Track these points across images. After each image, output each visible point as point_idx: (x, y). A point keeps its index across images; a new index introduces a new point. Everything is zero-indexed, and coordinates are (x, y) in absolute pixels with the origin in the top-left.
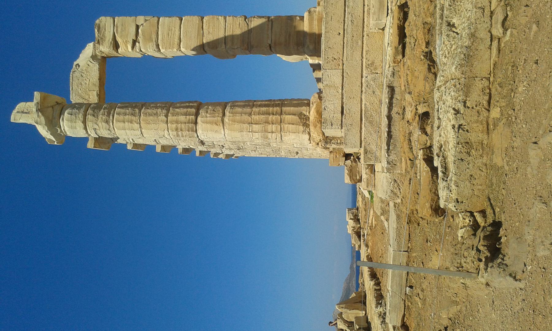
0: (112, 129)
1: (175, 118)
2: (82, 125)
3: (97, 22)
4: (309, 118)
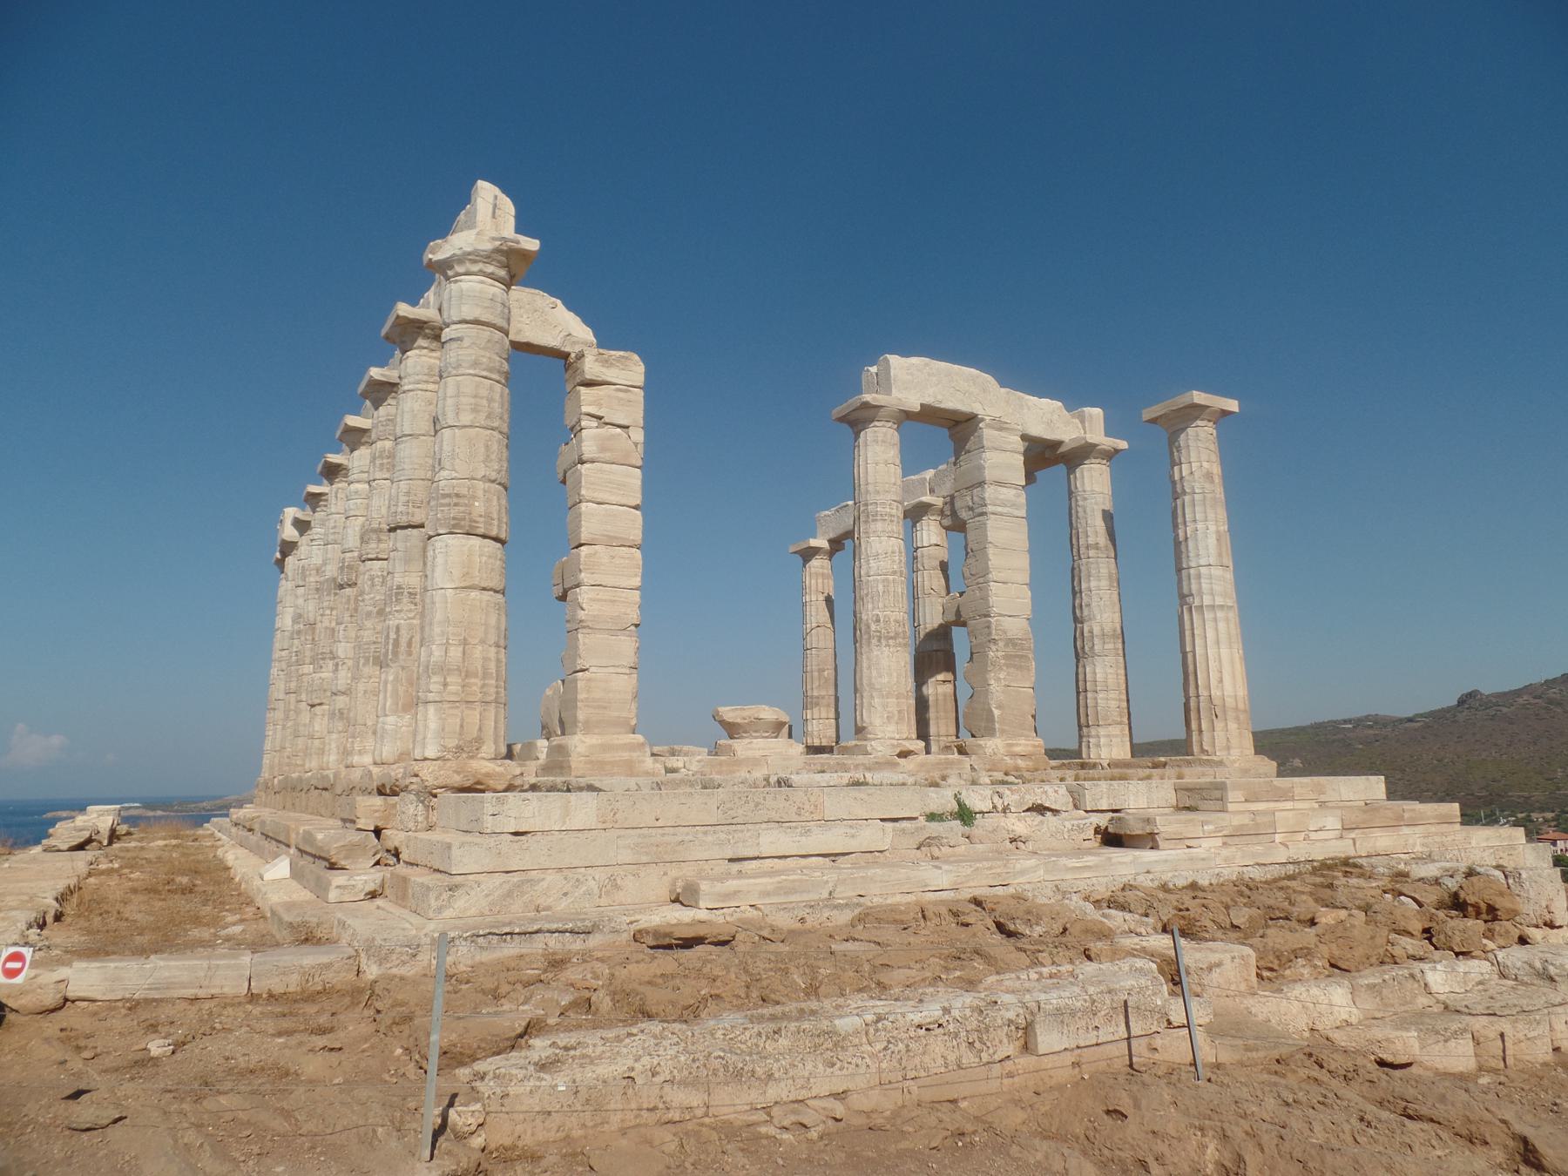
1: (480, 493)
3: (636, 357)
4: (472, 757)
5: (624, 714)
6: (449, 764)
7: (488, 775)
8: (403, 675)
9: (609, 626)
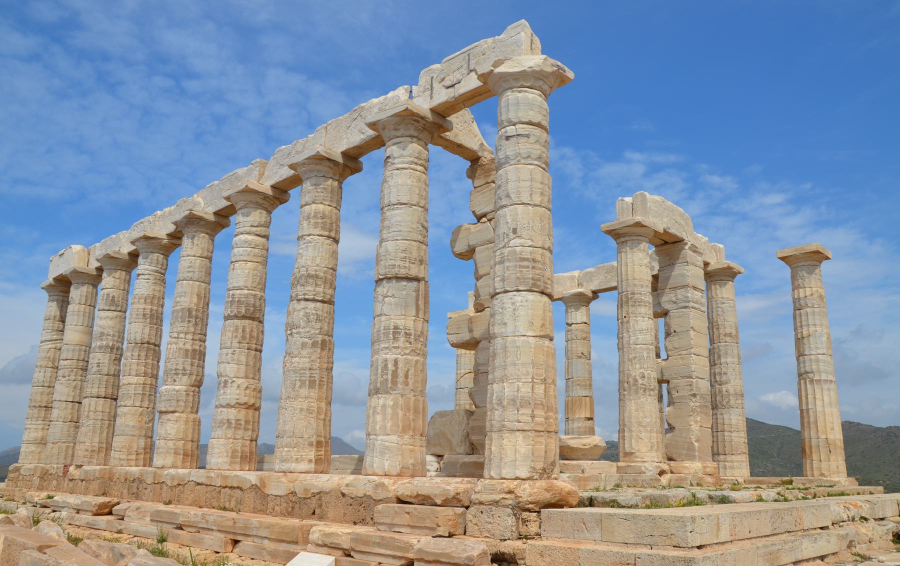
0: (530, 161)
1: (547, 261)
2: (536, 120)
4: (548, 478)
6: (539, 483)
7: (569, 493)
8: (401, 401)
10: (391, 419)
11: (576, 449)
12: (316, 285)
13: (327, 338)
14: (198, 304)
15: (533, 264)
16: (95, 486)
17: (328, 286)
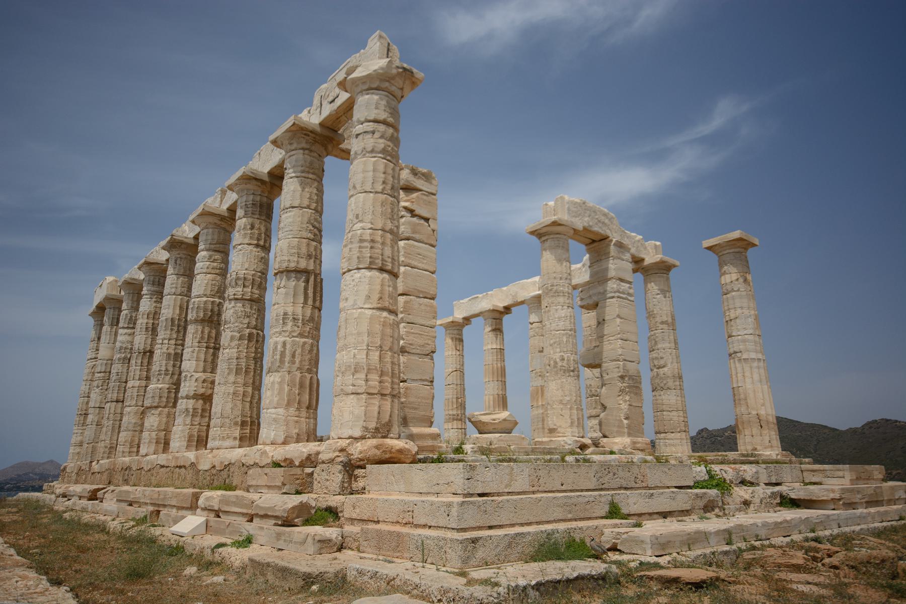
1: (388, 242)
5: (428, 414)
7: (400, 451)
8: (287, 377)
9: (418, 351)
10: (279, 394)
11: (487, 424)
12: (244, 286)
13: (254, 331)
14: (180, 315)
15: (372, 244)
16: (105, 476)
17: (255, 287)
